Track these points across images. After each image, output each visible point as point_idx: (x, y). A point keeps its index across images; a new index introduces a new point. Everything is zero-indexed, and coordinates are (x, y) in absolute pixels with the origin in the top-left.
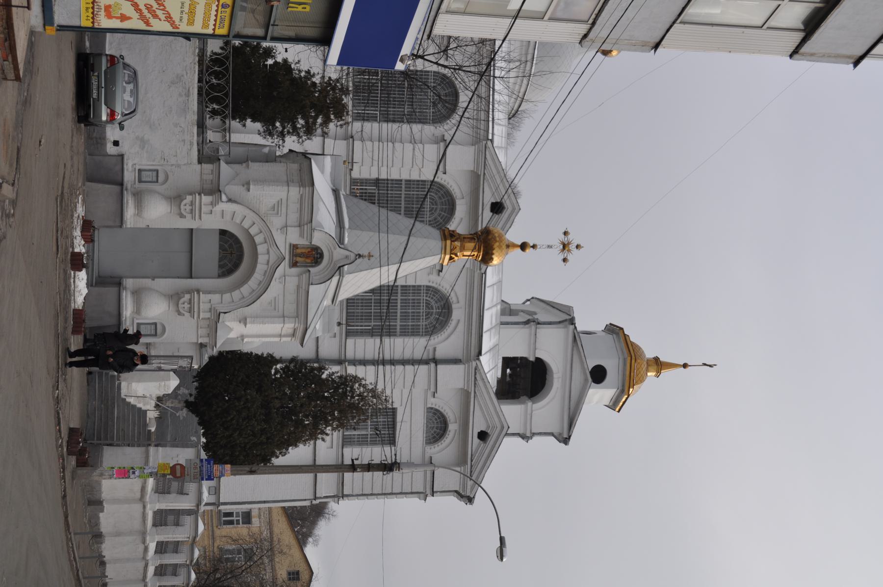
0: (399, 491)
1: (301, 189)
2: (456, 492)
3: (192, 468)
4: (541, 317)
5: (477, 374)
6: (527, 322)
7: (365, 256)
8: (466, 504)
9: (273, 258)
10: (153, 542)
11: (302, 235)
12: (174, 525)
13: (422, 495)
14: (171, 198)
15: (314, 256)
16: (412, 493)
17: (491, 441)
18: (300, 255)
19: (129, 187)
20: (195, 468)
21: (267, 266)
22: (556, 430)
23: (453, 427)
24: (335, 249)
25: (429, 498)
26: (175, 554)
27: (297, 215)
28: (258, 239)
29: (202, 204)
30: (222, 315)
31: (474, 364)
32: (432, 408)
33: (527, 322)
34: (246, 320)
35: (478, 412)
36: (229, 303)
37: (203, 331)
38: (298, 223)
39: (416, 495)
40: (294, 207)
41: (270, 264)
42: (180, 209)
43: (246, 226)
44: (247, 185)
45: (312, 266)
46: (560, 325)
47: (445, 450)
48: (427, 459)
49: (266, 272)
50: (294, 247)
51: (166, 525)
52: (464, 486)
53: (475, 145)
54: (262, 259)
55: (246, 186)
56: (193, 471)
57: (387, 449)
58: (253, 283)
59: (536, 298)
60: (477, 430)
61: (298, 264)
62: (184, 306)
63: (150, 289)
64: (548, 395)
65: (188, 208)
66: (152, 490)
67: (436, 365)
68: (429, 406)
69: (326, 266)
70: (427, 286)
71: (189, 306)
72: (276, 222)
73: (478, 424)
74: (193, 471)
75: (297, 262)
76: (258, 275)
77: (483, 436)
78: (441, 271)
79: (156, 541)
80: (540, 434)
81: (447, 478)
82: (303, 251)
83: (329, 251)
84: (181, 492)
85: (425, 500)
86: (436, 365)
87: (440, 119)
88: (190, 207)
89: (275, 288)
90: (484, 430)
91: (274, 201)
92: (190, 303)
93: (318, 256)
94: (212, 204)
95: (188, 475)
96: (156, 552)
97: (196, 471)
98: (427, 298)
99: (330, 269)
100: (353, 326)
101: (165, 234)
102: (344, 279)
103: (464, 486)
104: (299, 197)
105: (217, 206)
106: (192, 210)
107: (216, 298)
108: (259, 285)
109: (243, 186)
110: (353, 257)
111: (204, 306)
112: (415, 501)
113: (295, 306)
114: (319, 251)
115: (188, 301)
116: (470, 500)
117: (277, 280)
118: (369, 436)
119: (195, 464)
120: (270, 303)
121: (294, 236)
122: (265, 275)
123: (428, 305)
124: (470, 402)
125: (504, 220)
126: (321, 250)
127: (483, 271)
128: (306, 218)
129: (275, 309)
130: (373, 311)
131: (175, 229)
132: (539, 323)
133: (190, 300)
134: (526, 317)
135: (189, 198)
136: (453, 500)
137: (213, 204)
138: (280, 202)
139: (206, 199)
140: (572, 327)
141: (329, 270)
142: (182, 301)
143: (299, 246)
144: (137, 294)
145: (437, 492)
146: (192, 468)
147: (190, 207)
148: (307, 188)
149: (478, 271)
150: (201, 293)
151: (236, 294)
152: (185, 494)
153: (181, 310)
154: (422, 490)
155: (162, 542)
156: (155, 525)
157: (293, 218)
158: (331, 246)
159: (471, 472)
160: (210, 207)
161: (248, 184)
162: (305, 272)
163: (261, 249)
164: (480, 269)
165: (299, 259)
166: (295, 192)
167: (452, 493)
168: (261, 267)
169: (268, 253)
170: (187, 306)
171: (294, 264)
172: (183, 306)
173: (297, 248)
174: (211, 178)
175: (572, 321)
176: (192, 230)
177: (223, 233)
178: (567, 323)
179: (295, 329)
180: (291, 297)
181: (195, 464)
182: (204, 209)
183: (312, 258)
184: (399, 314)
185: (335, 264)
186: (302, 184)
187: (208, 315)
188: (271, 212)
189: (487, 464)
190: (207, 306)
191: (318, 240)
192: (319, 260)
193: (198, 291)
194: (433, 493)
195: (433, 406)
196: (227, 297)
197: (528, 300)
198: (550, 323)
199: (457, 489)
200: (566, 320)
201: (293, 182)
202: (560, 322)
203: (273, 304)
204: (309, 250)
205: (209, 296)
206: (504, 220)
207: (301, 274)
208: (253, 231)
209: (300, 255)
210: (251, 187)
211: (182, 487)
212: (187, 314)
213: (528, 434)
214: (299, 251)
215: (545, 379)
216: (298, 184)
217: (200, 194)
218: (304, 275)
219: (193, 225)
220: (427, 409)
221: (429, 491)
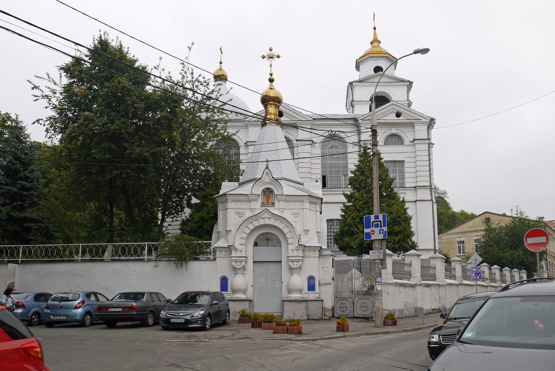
0: (428, 157)
1: (228, 201)
2: (428, 128)
3: (375, 255)
4: (351, 99)
5: (365, 119)
6: (352, 106)
7: (267, 164)
8: (435, 122)
9: (266, 215)
10: (445, 281)
11: (256, 200)
12: (435, 269)
13: (431, 146)
14: (236, 273)
15: (268, 192)
16: (429, 150)
17: (401, 110)
18: (268, 201)
19: (230, 297)
20: (375, 253)
21: (272, 219)
22: (405, 89)
23: (394, 131)
24: (263, 181)
25: (433, 141)
26: (456, 270)
27: (244, 203)
28: (256, 224)
29: (236, 256)
30: (300, 243)
31: (360, 121)
32: (384, 143)
33: (352, 106)
34: (304, 230)
35: (386, 118)
36: (293, 239)
37: (312, 254)
38: (249, 202)
39: (430, 149)
40: (239, 205)
41: (270, 216)
42: (240, 268)
43: (249, 231)
44: (228, 232)
45: (274, 193)
46: (353, 90)
47: (407, 135)
48: (411, 144)
49: (275, 219)
50: (263, 204)
51: (435, 274)
52: (424, 123)
53: (248, 127)
54: (268, 222)
55: (228, 232)
56: (377, 254)
57: (406, 165)
58: (281, 226)
59: (346, 107)
60: (396, 118)
61: (273, 202)
62: (295, 265)
63: (288, 285)
64: (389, 94)
65: (239, 264)
66: (408, 281)
67: (361, 141)
68: (383, 144)
69: (273, 186)
70: (321, 148)
71: (295, 262)
72: (248, 214)
73: (392, 117)
74: (377, 254)
75: (272, 203)
76: (276, 223)
77: (398, 115)
78: (312, 141)
79: (444, 279)
80: (408, 96)
81: (421, 131)
82: (265, 199)
83: (264, 185)
84: (410, 265)
85: (434, 144)
86: (361, 141)
87: (238, 147)
88: (238, 262)
89: (287, 215)
90: (395, 115)
91: (237, 216)
92: (294, 261)
93: (268, 191)
94: (236, 251)
95: (379, 257)
96: (455, 280)
97: (377, 252)
98: (328, 148)
99: (275, 184)
100: (343, 185)
101: (255, 276)
102: (284, 177)
103: (424, 123)
104: (233, 202)
105: (237, 248)
106: (240, 262)
107: (291, 247)
108: (283, 223)
109: (228, 234)
110: (267, 171)
111: (295, 253)
112: (434, 150)
113: (297, 203)
114: (266, 190)
115: (292, 263)
116: (432, 120)
117: (282, 213)
118: (400, 174)
119: (373, 253)
120: (296, 217)
121: (257, 206)
122: (277, 220)
123: (332, 147)
124: (380, 122)
125: (285, 110)
126: (265, 189)
127: (312, 119)
128: (245, 198)
129: (299, 214)
130: (335, 175)
131: (253, 271)
132: (353, 100)
133: (292, 261)
134: (351, 107)
135: (233, 263)
136: (433, 132)
137: (236, 250)
138: (237, 213)
139: (234, 254)
140: (354, 83)
141: (275, 184)
142: (293, 266)
143: (263, 202)
144: (290, 291)
145: (428, 137)
146: (375, 255)
147: (238, 262)
148: (228, 198)
149: (312, 121)
150: (288, 255)
151: (288, 236)
152: (411, 263)
153: (298, 266)
154: (427, 145)
155: (445, 276)
156: (435, 280)
157: (245, 205)
158: (261, 183)
159: (417, 120)
160: (238, 251)
161: (227, 231)
162: (277, 197)
163: (262, 222)
164: (311, 120)
165: (270, 202)
166: (230, 205)
167: (429, 130)
168: (272, 222)
169: (264, 218)
170: (295, 263)
171: (273, 204)
172: (295, 265)
173: (264, 203)
174: (224, 252)
175: (351, 84)
176: (254, 262)
177: (256, 244)
178: (352, 86)
179: (311, 202)
180: (291, 205)
181: (373, 253)
182: (239, 254)
183: (270, 194)
184: (336, 162)
185: (272, 181)
186: (226, 201)
187: (301, 251)
188: (243, 218)
189: (413, 111)
190: (295, 251)
191: (258, 190)
192: (271, 190)
193: (288, 257)
194: (429, 139)
195: (383, 142)
196: (290, 241)
197: (347, 110)
198: (353, 95)
199: (426, 127)
200: (351, 87)
201: (226, 206)
202: (352, 90)
203: (297, 215)
204: (265, 196)
205: (290, 251)
206: (285, 110)
207: (278, 199)
208: (252, 227)
209: (268, 201)
210: (228, 229)
211: (408, 264)
212: (300, 263)
213: (408, 102)
214: (265, 202)
215: (381, 96)
216: (227, 203)
217: (231, 257)
218: (278, 198)
219: (250, 261)
220: (385, 144)
221: (428, 141)
